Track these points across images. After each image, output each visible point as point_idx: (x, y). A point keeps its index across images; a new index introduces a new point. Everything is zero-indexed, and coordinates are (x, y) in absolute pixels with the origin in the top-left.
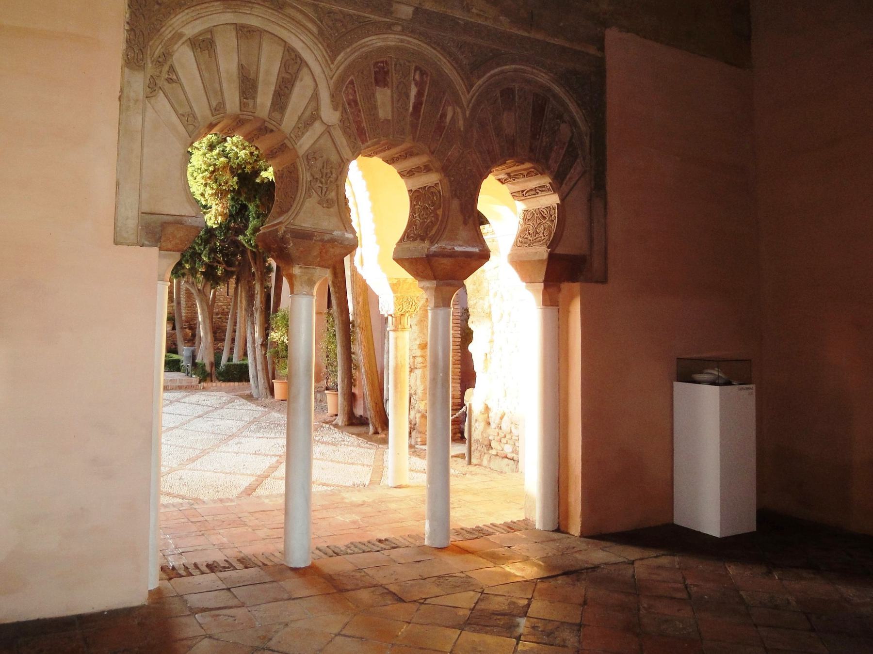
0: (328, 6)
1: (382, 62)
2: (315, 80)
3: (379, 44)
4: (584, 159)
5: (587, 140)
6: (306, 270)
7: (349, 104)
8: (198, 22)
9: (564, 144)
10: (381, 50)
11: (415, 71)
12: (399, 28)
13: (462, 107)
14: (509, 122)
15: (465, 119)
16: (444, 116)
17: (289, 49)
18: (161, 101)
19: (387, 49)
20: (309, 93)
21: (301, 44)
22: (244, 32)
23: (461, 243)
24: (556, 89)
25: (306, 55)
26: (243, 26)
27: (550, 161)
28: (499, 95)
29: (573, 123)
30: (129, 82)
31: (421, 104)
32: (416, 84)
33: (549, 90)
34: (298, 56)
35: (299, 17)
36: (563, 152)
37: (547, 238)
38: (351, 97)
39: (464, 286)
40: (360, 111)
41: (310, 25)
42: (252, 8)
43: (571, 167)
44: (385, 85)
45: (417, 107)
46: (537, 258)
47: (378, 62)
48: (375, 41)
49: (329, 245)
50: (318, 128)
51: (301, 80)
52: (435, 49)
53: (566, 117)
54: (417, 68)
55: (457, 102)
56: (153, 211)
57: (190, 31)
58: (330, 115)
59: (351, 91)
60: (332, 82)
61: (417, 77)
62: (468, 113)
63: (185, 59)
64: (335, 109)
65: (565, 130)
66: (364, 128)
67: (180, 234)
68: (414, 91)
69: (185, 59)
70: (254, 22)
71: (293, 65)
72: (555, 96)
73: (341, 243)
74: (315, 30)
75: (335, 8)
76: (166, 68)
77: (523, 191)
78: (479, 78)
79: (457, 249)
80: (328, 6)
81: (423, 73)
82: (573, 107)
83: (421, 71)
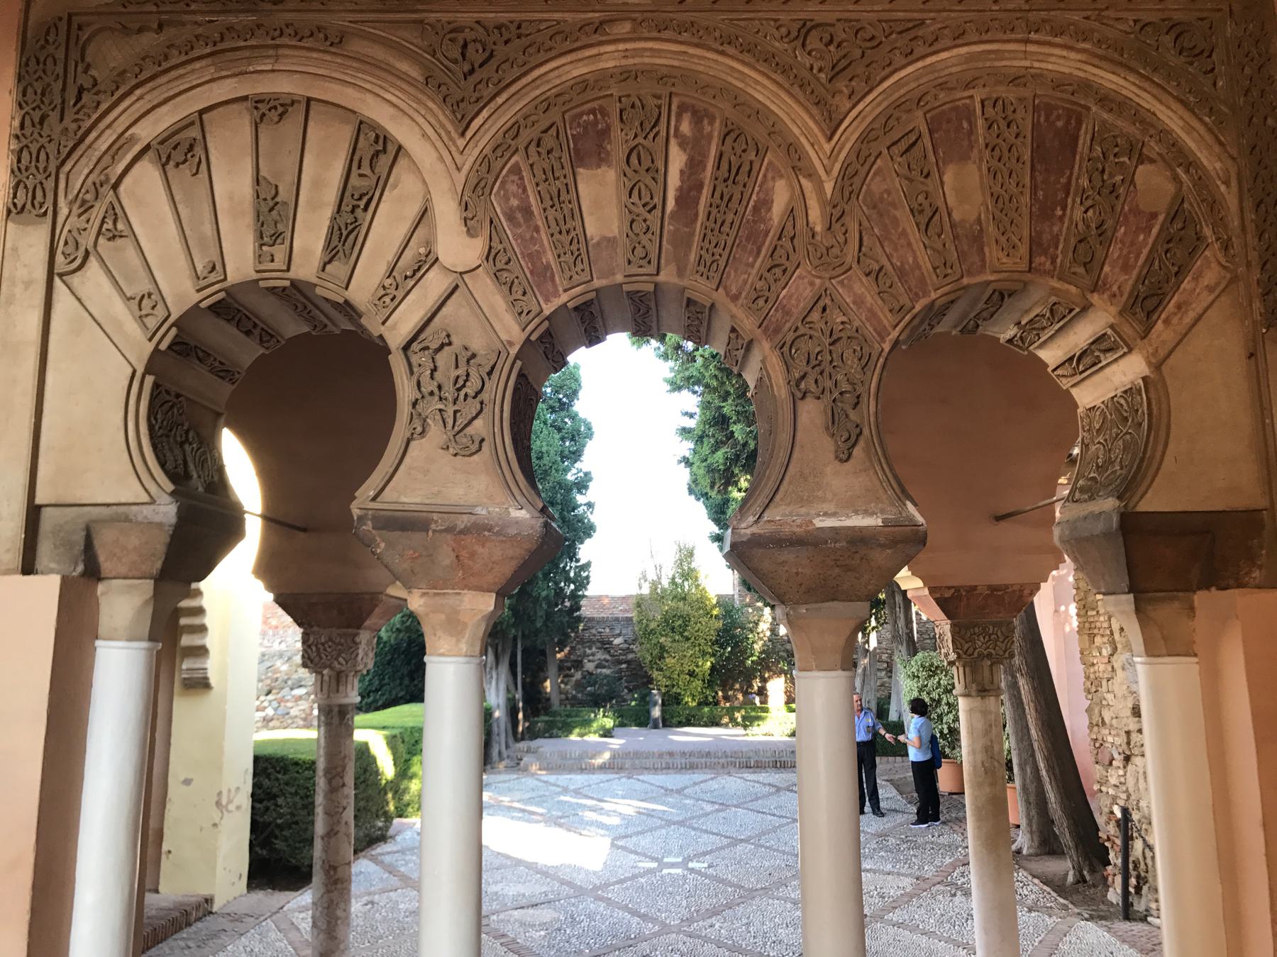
0: (445, 17)
1: (593, 111)
2: (424, 182)
3: (576, 73)
4: (1226, 247)
5: (1229, 196)
6: (438, 600)
7: (511, 218)
8: (164, 109)
9: (1154, 216)
10: (583, 85)
11: (679, 116)
12: (627, 26)
13: (811, 175)
14: (963, 188)
15: (823, 202)
16: (766, 203)
17: (362, 125)
18: (93, 280)
19: (603, 78)
20: (413, 210)
21: (392, 110)
22: (269, 110)
23: (830, 507)
24: (1110, 79)
25: (401, 131)
26: (258, 101)
27: (1107, 269)
28: (924, 129)
29: (1179, 157)
30: (15, 249)
31: (701, 186)
32: (682, 145)
33: (1086, 86)
34: (383, 140)
35: (379, 53)
36: (1147, 241)
37: (1124, 472)
38: (514, 202)
39: (1129, 592)
40: (537, 230)
41: (404, 66)
42: (277, 57)
43: (1180, 273)
44: (601, 158)
45: (687, 198)
46: (1099, 527)
47: (581, 115)
48: (568, 69)
49: (469, 540)
50: (435, 283)
51: (395, 187)
52: (723, 53)
53: (1153, 148)
54: (683, 108)
55: (798, 164)
56: (61, 501)
57: (147, 131)
58: (457, 248)
59: (513, 188)
60: (460, 178)
61: (685, 127)
62: (829, 187)
63: (145, 189)
64: (471, 233)
65: (1154, 185)
66: (548, 267)
67: (134, 541)
68: (677, 160)
69: (145, 189)
70: (284, 86)
71: (374, 154)
72: (1107, 100)
73: (498, 534)
74: (415, 73)
75: (465, 18)
76: (97, 213)
77: (1071, 359)
78: (855, 98)
79: (820, 523)
80: (445, 17)
81: (699, 117)
82: (1171, 118)
83: (695, 113)
